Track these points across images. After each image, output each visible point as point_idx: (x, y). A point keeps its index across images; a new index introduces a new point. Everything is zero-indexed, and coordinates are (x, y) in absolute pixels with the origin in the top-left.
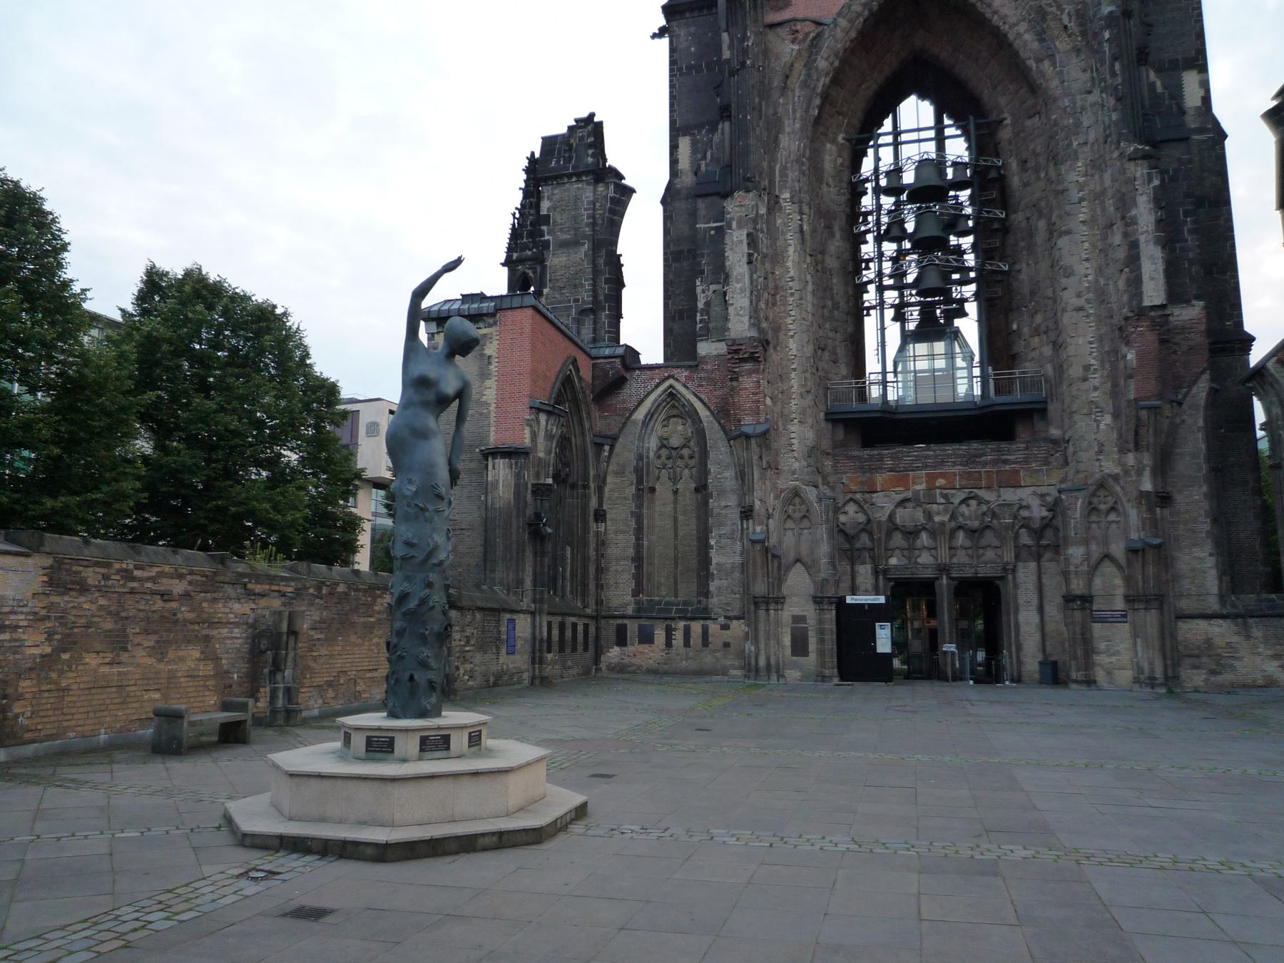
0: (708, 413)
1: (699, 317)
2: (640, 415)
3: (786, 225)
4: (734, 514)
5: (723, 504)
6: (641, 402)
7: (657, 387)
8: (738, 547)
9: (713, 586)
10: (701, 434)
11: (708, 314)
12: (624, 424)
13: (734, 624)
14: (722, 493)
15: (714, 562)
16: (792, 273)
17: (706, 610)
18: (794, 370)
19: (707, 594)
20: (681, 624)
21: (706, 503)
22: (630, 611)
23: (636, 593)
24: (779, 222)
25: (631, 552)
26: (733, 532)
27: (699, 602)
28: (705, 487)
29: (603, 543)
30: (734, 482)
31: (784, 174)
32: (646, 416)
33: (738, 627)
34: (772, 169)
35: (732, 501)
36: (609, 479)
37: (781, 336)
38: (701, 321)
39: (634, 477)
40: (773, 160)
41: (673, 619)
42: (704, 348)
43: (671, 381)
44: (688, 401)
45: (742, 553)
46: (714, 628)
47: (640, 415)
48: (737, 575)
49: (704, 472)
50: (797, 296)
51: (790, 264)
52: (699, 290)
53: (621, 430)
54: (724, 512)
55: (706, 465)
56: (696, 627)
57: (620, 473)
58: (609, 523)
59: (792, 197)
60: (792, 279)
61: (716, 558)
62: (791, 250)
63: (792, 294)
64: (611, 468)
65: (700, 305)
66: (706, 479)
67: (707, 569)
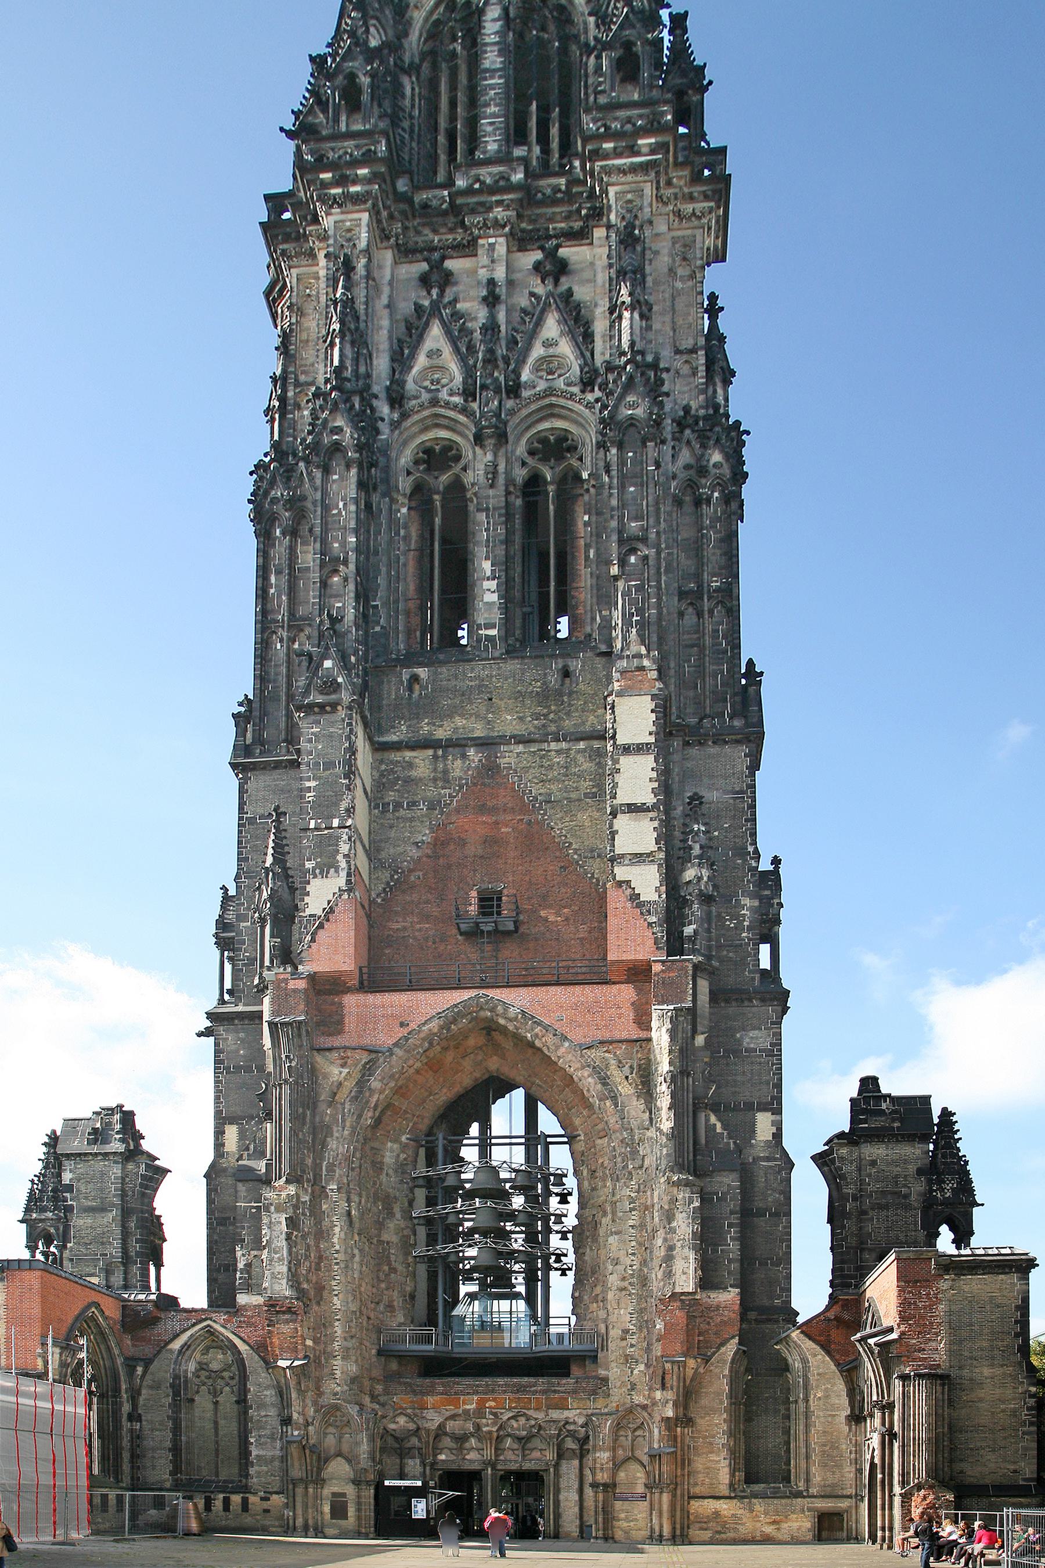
0: (247, 1348)
1: (238, 1275)
2: (176, 1345)
3: (333, 1209)
4: (275, 1422)
5: (263, 1414)
6: (176, 1336)
7: (194, 1325)
8: (278, 1444)
9: (252, 1471)
10: (240, 1362)
11: (248, 1272)
12: (159, 1352)
13: (275, 1497)
14: (262, 1406)
15: (254, 1453)
16: (337, 1247)
17: (246, 1486)
18: (339, 1320)
19: (247, 1476)
20: (221, 1496)
21: (246, 1413)
22: (168, 1485)
23: (173, 1473)
24: (324, 1207)
25: (168, 1444)
26: (273, 1434)
27: (240, 1481)
28: (245, 1401)
29: (138, 1437)
30: (274, 1399)
31: (331, 1168)
32: (182, 1347)
33: (277, 1500)
34: (317, 1167)
35: (273, 1412)
36: (144, 1392)
37: (325, 1294)
38: (240, 1278)
39: (170, 1391)
40: (319, 1156)
41: (212, 1492)
42: (242, 1299)
43: (209, 1322)
44: (227, 1338)
45: (282, 1449)
46: (252, 1499)
47: (176, 1345)
48: (277, 1463)
49: (243, 1391)
50: (342, 1266)
51: (335, 1240)
52: (239, 1254)
53: (155, 1356)
54: (264, 1419)
55: (245, 1385)
56: (236, 1499)
57: (156, 1386)
58: (144, 1423)
59: (339, 1189)
60: (337, 1252)
61: (255, 1452)
62: (337, 1230)
63: (337, 1264)
64: (144, 1383)
65: (241, 1265)
66: (246, 1396)
67: (247, 1459)
